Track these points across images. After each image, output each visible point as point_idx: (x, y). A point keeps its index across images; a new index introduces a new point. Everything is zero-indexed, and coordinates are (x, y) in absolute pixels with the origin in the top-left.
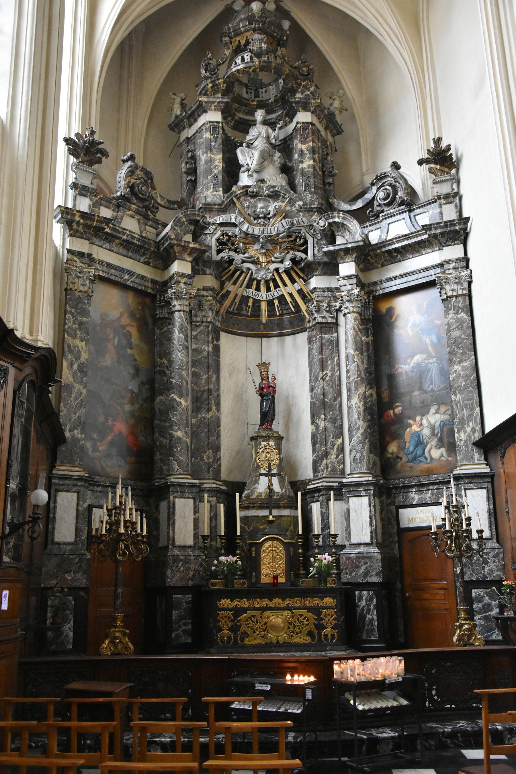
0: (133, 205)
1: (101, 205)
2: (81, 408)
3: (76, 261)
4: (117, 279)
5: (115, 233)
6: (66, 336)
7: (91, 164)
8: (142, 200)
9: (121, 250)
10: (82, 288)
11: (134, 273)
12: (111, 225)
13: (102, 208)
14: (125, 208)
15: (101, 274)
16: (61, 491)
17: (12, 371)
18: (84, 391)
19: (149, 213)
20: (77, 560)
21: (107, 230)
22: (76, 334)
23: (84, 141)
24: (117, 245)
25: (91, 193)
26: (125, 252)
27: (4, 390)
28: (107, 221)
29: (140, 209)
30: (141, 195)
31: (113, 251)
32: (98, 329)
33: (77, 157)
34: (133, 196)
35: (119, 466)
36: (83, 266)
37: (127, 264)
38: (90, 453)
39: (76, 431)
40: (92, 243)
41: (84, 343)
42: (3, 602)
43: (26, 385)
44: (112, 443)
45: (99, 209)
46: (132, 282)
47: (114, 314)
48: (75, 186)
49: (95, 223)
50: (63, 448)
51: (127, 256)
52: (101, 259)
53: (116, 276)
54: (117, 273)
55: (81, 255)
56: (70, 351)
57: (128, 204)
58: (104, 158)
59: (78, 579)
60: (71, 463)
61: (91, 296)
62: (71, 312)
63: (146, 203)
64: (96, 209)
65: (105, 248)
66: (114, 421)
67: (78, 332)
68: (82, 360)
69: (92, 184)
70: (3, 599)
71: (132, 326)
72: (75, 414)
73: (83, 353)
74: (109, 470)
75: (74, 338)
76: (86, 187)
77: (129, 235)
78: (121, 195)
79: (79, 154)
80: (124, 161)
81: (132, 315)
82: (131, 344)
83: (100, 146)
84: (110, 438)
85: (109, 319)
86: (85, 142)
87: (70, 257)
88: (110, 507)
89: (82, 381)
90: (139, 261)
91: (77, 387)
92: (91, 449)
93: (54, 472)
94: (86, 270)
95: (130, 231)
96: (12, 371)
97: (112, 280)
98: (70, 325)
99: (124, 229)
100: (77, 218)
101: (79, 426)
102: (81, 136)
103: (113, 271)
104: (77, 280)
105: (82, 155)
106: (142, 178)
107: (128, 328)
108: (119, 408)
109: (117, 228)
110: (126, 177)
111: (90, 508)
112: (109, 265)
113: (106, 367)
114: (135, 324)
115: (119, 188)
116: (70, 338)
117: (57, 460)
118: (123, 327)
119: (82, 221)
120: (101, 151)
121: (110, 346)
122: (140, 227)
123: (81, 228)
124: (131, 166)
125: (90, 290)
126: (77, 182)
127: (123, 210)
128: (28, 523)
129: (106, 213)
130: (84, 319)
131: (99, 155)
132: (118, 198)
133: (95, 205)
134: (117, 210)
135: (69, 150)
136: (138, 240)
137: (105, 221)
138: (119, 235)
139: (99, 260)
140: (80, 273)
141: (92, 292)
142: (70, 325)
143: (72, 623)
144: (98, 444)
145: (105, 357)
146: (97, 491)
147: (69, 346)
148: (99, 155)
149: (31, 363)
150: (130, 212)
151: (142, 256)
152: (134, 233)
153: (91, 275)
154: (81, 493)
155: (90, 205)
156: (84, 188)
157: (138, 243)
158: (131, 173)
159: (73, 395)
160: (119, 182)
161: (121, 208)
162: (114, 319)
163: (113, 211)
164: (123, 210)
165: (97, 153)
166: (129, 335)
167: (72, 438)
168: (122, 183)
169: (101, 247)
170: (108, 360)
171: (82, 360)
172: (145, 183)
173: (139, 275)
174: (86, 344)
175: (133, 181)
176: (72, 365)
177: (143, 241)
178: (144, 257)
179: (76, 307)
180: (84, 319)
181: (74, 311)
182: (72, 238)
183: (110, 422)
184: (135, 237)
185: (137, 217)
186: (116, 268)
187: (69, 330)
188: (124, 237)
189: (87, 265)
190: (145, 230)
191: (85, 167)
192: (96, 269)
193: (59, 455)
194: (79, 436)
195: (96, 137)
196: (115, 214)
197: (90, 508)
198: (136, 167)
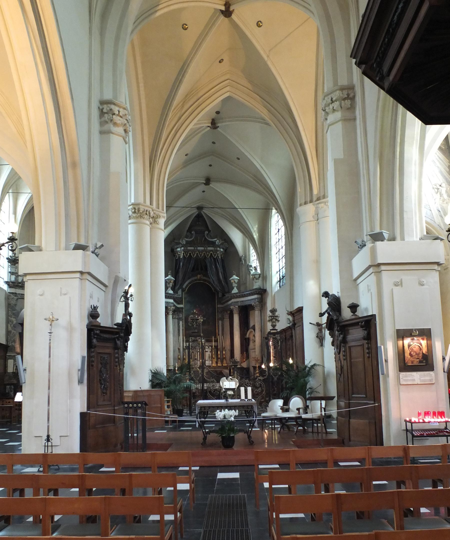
10: (13, 303)
15: (19, 297)
55: (13, 293)
60: (12, 352)
68: (14, 323)
75: (11, 317)
91: (13, 331)
130: (14, 312)
135: (8, 261)
156: (13, 273)
159: (12, 333)
171: (14, 323)
176: (11, 325)
180: (14, 312)
181: (11, 310)
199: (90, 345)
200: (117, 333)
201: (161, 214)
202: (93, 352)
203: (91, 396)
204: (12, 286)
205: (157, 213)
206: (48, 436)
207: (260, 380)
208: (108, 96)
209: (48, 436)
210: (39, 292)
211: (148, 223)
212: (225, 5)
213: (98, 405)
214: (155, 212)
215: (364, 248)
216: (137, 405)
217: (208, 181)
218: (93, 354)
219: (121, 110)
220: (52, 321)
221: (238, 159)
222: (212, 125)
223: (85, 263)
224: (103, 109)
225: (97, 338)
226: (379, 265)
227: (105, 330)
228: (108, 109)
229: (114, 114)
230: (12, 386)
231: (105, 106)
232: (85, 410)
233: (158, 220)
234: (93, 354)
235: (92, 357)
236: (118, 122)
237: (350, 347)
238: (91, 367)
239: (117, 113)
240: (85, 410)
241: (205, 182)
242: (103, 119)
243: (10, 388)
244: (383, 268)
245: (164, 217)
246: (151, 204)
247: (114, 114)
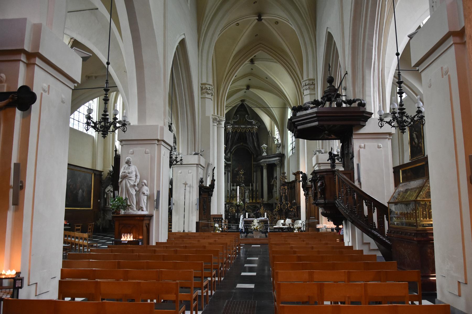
199: (200, 194)
200: (210, 189)
201: (223, 119)
202: (201, 197)
203: (200, 215)
205: (221, 119)
206: (184, 230)
207: (275, 211)
208: (204, 81)
209: (184, 230)
210: (180, 171)
211: (216, 124)
212: (258, 16)
213: (202, 219)
214: (219, 118)
215: (315, 155)
216: (219, 219)
217: (248, 87)
218: (201, 198)
219: (211, 87)
220: (186, 184)
221: (267, 78)
222: (251, 62)
223: (199, 160)
224: (202, 87)
225: (202, 191)
226: (320, 163)
227: (206, 188)
228: (205, 87)
229: (207, 89)
231: (203, 86)
232: (198, 221)
233: (221, 122)
234: (201, 198)
235: (201, 199)
236: (209, 93)
237: (310, 197)
238: (200, 203)
239: (209, 89)
240: (198, 221)
241: (246, 88)
242: (202, 91)
244: (321, 165)
245: (224, 120)
246: (217, 115)
247: (207, 89)
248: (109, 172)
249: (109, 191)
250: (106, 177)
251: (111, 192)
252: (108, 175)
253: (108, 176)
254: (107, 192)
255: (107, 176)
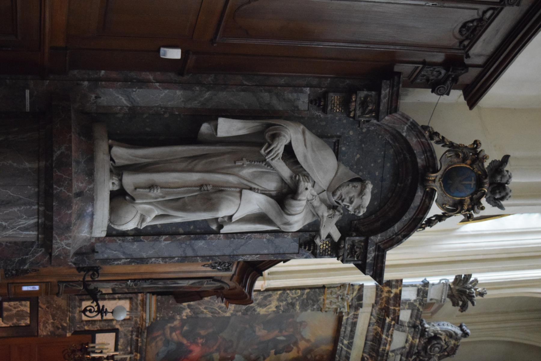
0: (418, 340)
1: (413, 310)
2: (212, 313)
3: (353, 294)
4: (342, 333)
5: (386, 327)
6: (279, 292)
7: (451, 296)
8: (425, 349)
9: (372, 334)
10: (327, 302)
11: (351, 349)
12: (393, 323)
13: (409, 312)
14: (414, 334)
15: (345, 318)
16: (131, 303)
17: (229, 274)
18: (228, 314)
19: (414, 357)
20: (65, 325)
21: (388, 320)
22: (282, 301)
23: (471, 288)
24: (376, 329)
25: (422, 300)
26: (370, 337)
27: (211, 270)
28: (396, 319)
29: (416, 348)
30: (429, 347)
31: (369, 326)
32: (290, 320)
33: (454, 283)
34: (427, 340)
35: (157, 354)
36: (350, 300)
37: (359, 341)
38: (169, 325)
39: (188, 310)
40: (373, 306)
41: (275, 309)
42: (29, 287)
43: (218, 284)
44: (180, 344)
45: (408, 309)
46: (342, 348)
47: (307, 333)
48: (426, 284)
49: (392, 308)
50: (172, 301)
51: (366, 340)
52: (359, 316)
53: (345, 332)
54: (348, 332)
55: (360, 298)
56: (265, 298)
57: (419, 336)
58: (459, 308)
59: (46, 327)
60: (158, 309)
61: (321, 310)
62: (303, 294)
63: (422, 353)
64: (407, 306)
65: (370, 319)
66: (202, 344)
67: (284, 303)
69: (431, 299)
70: (31, 287)
71: (298, 352)
72: (205, 308)
73: (265, 309)
74: (154, 344)
75: (279, 300)
76: (427, 295)
77: (387, 340)
78: (426, 328)
79: (457, 285)
80: (461, 327)
81: (309, 351)
82: (281, 353)
83: (470, 303)
84: (185, 342)
85: (301, 330)
86: (470, 289)
87: (357, 288)
88: (116, 357)
89: (237, 311)
90: (364, 352)
92: (172, 325)
93: (148, 295)
94: (346, 304)
95: (391, 342)
96: (229, 274)
97: (341, 328)
98: (291, 295)
99: (392, 335)
100: (394, 291)
101: (194, 313)
102: (475, 285)
103: (349, 329)
104: (335, 296)
105: (457, 288)
106: (448, 346)
107: (295, 348)
108: (215, 348)
109: (392, 329)
110: (444, 331)
111: (116, 331)
112: (354, 324)
113: (254, 332)
114: (301, 354)
115: (433, 325)
116: (278, 296)
117: (160, 297)
118: (296, 343)
119: (392, 295)
120: (465, 304)
121: (276, 332)
122: (398, 350)
123: (385, 295)
124: (456, 334)
125: (327, 309)
126: (430, 286)
127: (412, 332)
128: (98, 305)
129: (405, 315)
130: (298, 307)
131: (461, 303)
132: (423, 326)
133: (411, 305)
134: (411, 325)
136: (384, 350)
137: (395, 317)
138: (385, 331)
139: (357, 315)
140: (342, 299)
141: (326, 312)
142: (291, 295)
143: (4, 325)
144: (178, 332)
145: (264, 329)
146: (132, 335)
147: (270, 296)
148: (461, 303)
149: (239, 287)
150: (410, 338)
151: (369, 355)
152: (390, 345)
153: (342, 309)
154: (129, 322)
155: (410, 300)
156: (426, 293)
157: (381, 350)
158: (450, 335)
160: (439, 325)
161: (413, 330)
162: (303, 333)
163: (409, 322)
164: (412, 332)
165: (461, 301)
166: (288, 349)
167: (181, 308)
168: (438, 328)
169: (371, 315)
170: (261, 332)
172: (442, 350)
173: (350, 354)
174: (274, 311)
175: (443, 339)
177: (384, 355)
178: (368, 357)
179: (307, 299)
180: (298, 307)
181: (305, 296)
182: (375, 287)
183: (200, 341)
184: (386, 346)
185: (407, 345)
186: (353, 331)
187: (285, 295)
188: (384, 336)
189: (350, 304)
190: (397, 354)
191: (446, 291)
192: (348, 314)
193: (164, 298)
194: (184, 314)
195: (477, 298)
196: (406, 324)
197: (116, 331)
198: (457, 339)
204: (385, 295)
230: (28, 322)
243: (20, 315)
248: (486, 164)
249: (285, 171)
250: (433, 134)
251: (272, 185)
252: (452, 145)
253: (439, 150)
254: (279, 147)
255: (442, 141)
